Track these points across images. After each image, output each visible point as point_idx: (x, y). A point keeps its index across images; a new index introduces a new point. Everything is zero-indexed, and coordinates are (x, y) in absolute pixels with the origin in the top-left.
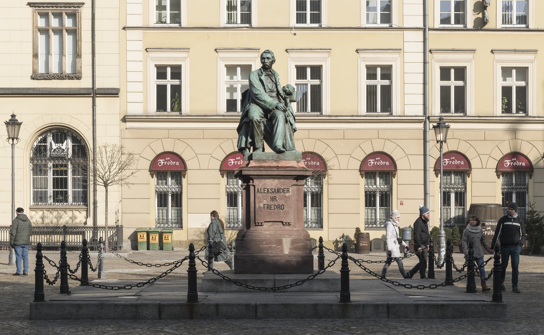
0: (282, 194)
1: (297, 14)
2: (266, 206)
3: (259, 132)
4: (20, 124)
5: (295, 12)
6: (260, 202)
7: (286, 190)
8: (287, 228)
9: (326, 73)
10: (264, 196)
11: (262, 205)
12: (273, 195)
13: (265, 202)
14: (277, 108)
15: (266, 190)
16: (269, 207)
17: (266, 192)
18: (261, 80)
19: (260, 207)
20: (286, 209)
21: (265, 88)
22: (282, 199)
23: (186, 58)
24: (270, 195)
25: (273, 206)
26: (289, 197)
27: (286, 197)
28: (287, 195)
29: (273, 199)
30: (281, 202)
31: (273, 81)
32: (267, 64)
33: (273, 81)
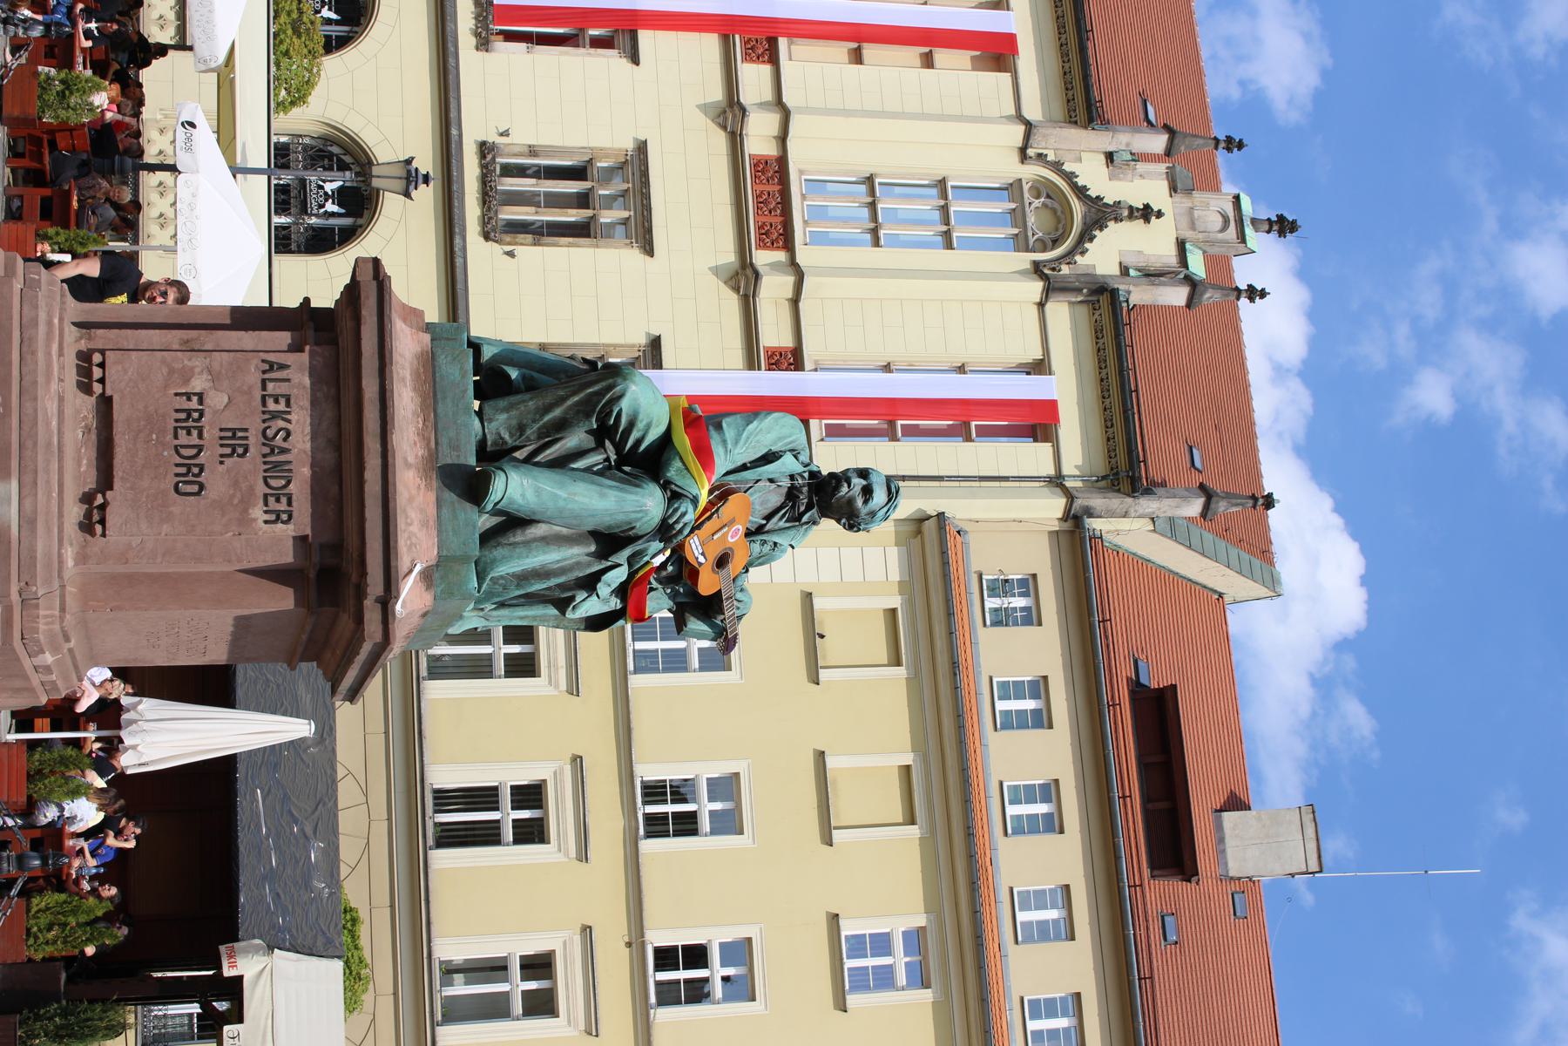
0: (261, 489)
1: (676, 947)
2: (194, 404)
3: (557, 412)
4: (407, 195)
5: (680, 944)
6: (215, 377)
7: (283, 506)
8: (75, 512)
9: (540, 1026)
10: (249, 392)
11: (197, 385)
12: (254, 440)
13: (217, 400)
14: (675, 496)
15: (282, 407)
16: (190, 419)
17: (272, 406)
18: (769, 458)
19: (187, 376)
20: (179, 505)
21: (744, 468)
22: (236, 484)
23: (557, 686)
24: (255, 425)
25: (197, 442)
26: (245, 521)
27: (246, 504)
28: (258, 513)
29: (234, 442)
30: (217, 479)
31: (768, 518)
32: (845, 489)
33: (768, 518)
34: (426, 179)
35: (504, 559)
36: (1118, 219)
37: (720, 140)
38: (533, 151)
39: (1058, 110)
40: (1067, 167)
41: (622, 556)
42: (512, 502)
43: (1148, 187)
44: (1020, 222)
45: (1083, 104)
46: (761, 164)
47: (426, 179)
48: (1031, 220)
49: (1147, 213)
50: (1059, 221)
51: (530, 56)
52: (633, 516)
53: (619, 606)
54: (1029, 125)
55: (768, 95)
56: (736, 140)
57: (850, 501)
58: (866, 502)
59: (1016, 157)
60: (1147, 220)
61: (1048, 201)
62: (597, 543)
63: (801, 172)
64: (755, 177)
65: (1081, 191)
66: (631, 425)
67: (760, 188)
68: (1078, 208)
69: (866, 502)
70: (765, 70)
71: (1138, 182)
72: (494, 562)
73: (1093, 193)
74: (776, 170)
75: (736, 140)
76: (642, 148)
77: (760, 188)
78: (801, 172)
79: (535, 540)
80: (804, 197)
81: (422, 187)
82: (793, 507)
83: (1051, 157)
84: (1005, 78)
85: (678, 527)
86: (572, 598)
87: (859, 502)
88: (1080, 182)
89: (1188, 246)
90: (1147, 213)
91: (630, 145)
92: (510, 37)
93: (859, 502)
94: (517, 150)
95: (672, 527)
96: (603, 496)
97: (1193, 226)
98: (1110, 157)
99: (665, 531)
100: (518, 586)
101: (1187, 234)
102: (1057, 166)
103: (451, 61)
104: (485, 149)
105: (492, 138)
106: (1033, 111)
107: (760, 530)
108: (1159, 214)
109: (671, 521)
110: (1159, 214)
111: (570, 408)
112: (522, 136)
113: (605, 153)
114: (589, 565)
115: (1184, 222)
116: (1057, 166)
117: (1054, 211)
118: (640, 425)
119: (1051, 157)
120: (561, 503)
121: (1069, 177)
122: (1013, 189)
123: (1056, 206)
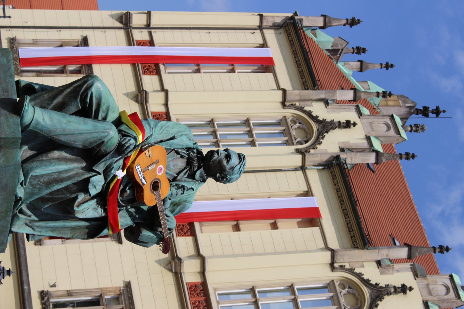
31: (178, 174)
32: (216, 156)
33: (178, 174)
34: (9, 273)
35: (37, 167)
36: (389, 294)
37: (169, 277)
38: (69, 294)
39: (347, 241)
40: (357, 271)
41: (100, 167)
42: (38, 123)
43: (403, 276)
44: (336, 302)
45: (359, 236)
46: (193, 287)
47: (9, 273)
48: (342, 301)
49: (404, 289)
50: (357, 300)
51: (64, 245)
52: (102, 135)
53: (103, 215)
54: (333, 252)
55: (192, 251)
56: (178, 276)
57: (220, 162)
58: (228, 162)
59: (328, 269)
60: (405, 293)
61: (350, 290)
62: (86, 162)
63: (215, 290)
64: (191, 294)
65: (367, 282)
66: (99, 105)
67: (194, 299)
68: (366, 291)
69: (228, 162)
70: (190, 239)
71: (396, 274)
72: (32, 169)
73: (373, 282)
74: (202, 289)
75: (178, 276)
76: (128, 286)
77: (194, 299)
78: (215, 290)
79: (53, 159)
80: (218, 303)
81: (7, 277)
82: (190, 169)
83: (347, 266)
84: (316, 230)
85: (127, 145)
86: (76, 198)
87: (225, 162)
88: (365, 277)
89: (430, 304)
90: (404, 289)
91: (121, 285)
92: (51, 238)
93: (225, 162)
94: (60, 293)
95: (124, 145)
96: (85, 123)
97: (430, 293)
98: (379, 263)
99: (120, 150)
100: (47, 188)
101: (428, 298)
102: (351, 271)
103: (22, 251)
104: (43, 295)
105: (46, 288)
106: (334, 244)
107: (175, 179)
108: (411, 289)
109: (123, 143)
110: (411, 289)
111: (66, 96)
112: (62, 287)
113: (108, 290)
114: (83, 174)
115: (425, 292)
116: (351, 271)
117: (354, 295)
118: (103, 107)
119: (347, 266)
120: (64, 126)
121: (359, 276)
122: (329, 286)
123: (355, 292)
